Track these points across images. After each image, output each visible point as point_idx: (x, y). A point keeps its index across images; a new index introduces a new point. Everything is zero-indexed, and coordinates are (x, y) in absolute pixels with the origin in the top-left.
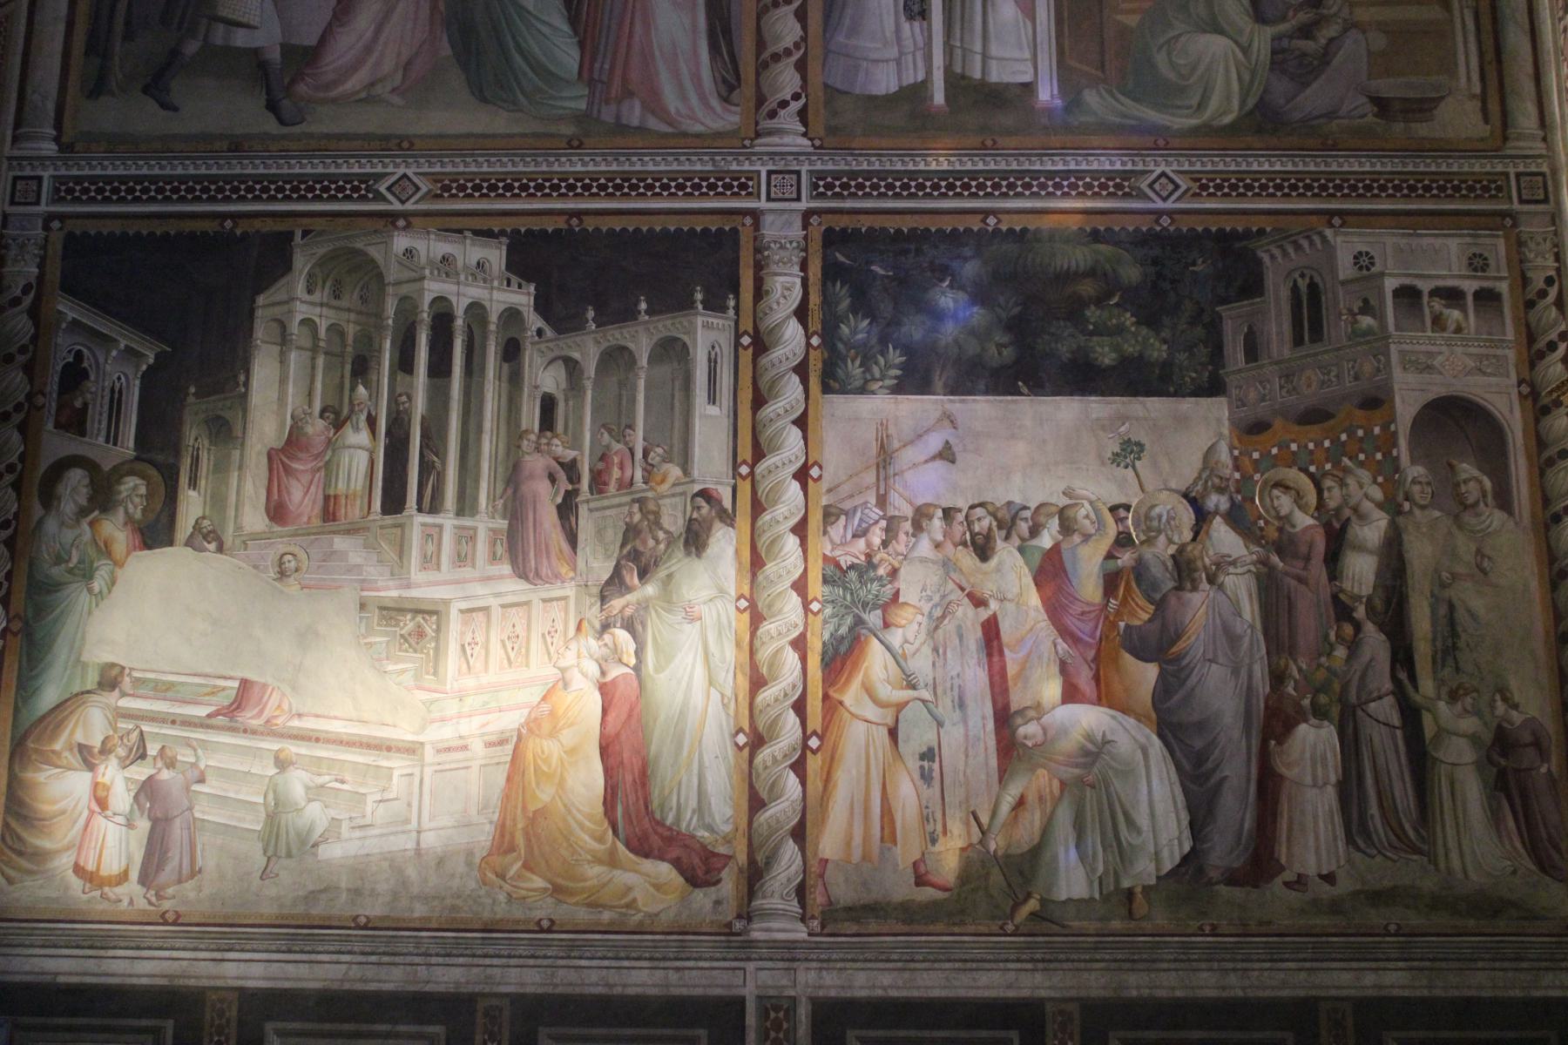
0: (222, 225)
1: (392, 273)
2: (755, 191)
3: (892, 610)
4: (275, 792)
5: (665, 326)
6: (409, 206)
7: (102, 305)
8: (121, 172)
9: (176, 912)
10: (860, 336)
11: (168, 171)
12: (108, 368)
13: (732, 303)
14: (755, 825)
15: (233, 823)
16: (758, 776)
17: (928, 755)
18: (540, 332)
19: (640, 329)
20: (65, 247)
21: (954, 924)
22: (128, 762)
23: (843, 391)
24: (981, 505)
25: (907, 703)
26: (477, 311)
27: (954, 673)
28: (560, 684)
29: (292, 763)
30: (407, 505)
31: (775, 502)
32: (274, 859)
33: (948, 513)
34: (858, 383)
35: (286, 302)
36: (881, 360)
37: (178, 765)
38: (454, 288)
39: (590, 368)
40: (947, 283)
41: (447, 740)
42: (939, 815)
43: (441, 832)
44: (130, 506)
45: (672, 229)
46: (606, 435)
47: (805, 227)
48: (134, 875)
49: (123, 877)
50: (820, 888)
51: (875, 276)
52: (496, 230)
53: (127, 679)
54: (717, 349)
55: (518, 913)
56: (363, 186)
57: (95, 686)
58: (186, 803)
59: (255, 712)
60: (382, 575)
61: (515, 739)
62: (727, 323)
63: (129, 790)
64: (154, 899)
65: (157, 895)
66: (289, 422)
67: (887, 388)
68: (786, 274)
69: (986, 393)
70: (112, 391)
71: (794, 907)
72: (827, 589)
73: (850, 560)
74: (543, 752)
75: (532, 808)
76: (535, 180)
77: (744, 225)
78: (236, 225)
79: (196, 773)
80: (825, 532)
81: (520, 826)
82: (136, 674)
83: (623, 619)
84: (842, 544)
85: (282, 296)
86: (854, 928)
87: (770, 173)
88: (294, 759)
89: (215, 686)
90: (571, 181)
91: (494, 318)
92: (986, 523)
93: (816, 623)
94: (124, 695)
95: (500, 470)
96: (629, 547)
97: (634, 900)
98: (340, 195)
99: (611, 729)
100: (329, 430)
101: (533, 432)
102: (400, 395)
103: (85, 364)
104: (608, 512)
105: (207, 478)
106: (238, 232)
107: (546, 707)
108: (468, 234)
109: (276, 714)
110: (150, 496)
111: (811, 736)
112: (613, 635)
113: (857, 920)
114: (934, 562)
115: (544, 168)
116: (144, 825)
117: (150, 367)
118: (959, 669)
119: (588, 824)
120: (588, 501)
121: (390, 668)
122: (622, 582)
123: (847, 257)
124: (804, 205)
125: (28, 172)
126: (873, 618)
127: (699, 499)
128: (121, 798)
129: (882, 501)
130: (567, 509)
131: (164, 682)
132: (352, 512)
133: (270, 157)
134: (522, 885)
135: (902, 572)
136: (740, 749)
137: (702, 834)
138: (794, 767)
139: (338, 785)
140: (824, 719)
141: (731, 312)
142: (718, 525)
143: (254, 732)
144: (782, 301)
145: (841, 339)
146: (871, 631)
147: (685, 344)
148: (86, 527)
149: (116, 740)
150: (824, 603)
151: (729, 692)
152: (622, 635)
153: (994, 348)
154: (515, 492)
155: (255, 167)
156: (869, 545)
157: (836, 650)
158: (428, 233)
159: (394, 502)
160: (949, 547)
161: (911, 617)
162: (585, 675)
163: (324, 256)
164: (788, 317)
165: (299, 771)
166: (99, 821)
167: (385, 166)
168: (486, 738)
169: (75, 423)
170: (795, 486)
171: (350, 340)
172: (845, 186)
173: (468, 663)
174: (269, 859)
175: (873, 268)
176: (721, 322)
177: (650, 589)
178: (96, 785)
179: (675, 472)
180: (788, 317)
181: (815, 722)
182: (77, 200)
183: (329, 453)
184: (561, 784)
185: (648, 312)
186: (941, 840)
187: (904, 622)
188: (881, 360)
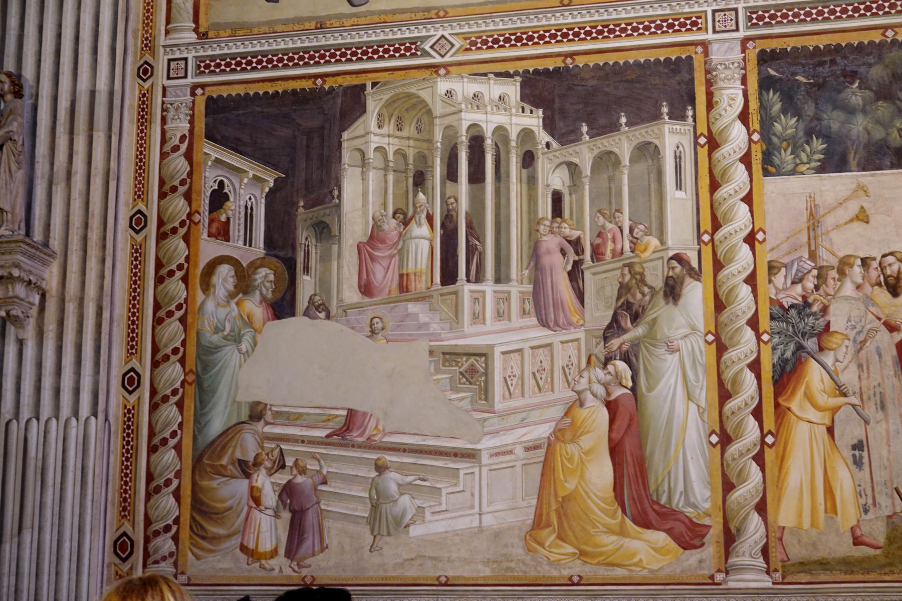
0: (314, 83)
1: (438, 109)
2: (704, 26)
3: (825, 337)
5: (640, 134)
6: (447, 59)
7: (236, 147)
8: (241, 50)
9: (312, 577)
10: (789, 131)
11: (274, 47)
12: (242, 192)
13: (690, 113)
14: (727, 503)
16: (728, 465)
17: (858, 446)
18: (548, 145)
19: (623, 137)
20: (207, 107)
21: (885, 574)
22: (273, 471)
23: (779, 174)
24: (891, 254)
25: (840, 407)
26: (500, 131)
27: (876, 383)
28: (578, 403)
31: (731, 261)
32: (378, 537)
33: (865, 262)
34: (790, 167)
35: (363, 136)
36: (807, 148)
37: (308, 472)
39: (587, 170)
40: (856, 85)
41: (498, 447)
42: (869, 491)
44: (264, 289)
45: (642, 60)
46: (601, 218)
47: (743, 51)
48: (282, 551)
49: (274, 553)
50: (780, 549)
51: (799, 84)
52: (512, 72)
53: (269, 413)
54: (681, 148)
55: (555, 573)
56: (411, 47)
57: (247, 418)
58: (315, 499)
59: (360, 431)
60: (443, 329)
61: (546, 445)
62: (687, 128)
63: (275, 491)
64: (296, 568)
65: (298, 564)
66: (371, 222)
67: (813, 169)
68: (730, 88)
69: (892, 167)
70: (246, 207)
71: (760, 562)
72: (774, 324)
73: (791, 301)
74: (567, 453)
75: (562, 493)
77: (696, 53)
78: (324, 82)
79: (321, 477)
80: (770, 281)
81: (554, 506)
82: (274, 409)
83: (621, 353)
84: (783, 289)
85: (361, 131)
86: (807, 578)
87: (714, 11)
88: (389, 464)
89: (330, 415)
91: (513, 136)
92: (895, 268)
93: (766, 351)
94: (267, 423)
95: (525, 248)
96: (622, 300)
97: (641, 560)
98: (397, 55)
99: (616, 436)
101: (547, 219)
102: (449, 198)
103: (226, 190)
106: (326, 87)
107: (568, 420)
108: (492, 76)
109: (375, 432)
110: (276, 282)
111: (766, 435)
112: (614, 365)
113: (809, 572)
114: (854, 298)
115: (544, 22)
116: (286, 515)
117: (270, 189)
118: (880, 380)
121: (454, 396)
122: (619, 326)
123: (777, 71)
124: (742, 34)
125: (177, 55)
126: (811, 344)
127: (674, 262)
128: (270, 498)
129: (813, 256)
130: (575, 274)
131: (295, 414)
132: (419, 285)
133: (345, 31)
134: (556, 551)
135: (832, 309)
136: (714, 446)
137: (689, 511)
138: (754, 458)
140: (776, 422)
141: (690, 120)
142: (688, 280)
144: (728, 108)
145: (775, 134)
146: (809, 353)
147: (656, 146)
148: (233, 304)
149: (264, 456)
150: (772, 334)
151: (703, 404)
152: (622, 365)
153: (896, 132)
154: (536, 264)
155: (335, 39)
156: (804, 289)
157: (783, 369)
158: (462, 77)
159: (449, 276)
160: (868, 289)
161: (840, 342)
162: (595, 396)
163: (387, 101)
164: (734, 121)
166: (256, 513)
167: (428, 30)
169: (222, 233)
170: (746, 248)
171: (411, 161)
172: (773, 17)
173: (509, 389)
174: (375, 537)
175: (797, 78)
176: (683, 128)
177: (639, 331)
178: (252, 488)
179: (654, 242)
180: (734, 121)
181: (769, 423)
182: (213, 72)
183: (401, 243)
184: (582, 477)
185: (629, 124)
186: (872, 510)
187: (834, 346)
188: (807, 148)
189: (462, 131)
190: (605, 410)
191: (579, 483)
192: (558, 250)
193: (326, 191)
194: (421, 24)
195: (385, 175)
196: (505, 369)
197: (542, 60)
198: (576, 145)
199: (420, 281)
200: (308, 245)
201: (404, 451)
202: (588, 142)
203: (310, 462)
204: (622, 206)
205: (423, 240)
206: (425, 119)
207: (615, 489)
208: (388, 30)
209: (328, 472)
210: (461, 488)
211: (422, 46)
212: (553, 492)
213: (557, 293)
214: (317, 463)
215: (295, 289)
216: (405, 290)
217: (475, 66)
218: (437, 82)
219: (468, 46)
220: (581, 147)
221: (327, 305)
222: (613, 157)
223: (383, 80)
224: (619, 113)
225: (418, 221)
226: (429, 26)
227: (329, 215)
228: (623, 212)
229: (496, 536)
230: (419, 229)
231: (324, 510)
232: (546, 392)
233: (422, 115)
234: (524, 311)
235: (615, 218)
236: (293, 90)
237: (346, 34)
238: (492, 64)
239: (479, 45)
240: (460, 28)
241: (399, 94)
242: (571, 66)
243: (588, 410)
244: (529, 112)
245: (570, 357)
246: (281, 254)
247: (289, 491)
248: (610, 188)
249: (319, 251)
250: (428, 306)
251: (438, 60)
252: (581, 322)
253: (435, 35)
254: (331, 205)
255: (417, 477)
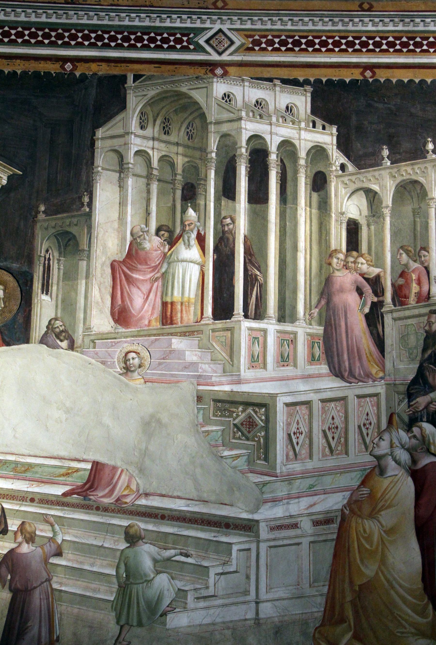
0: (62, 67)
4: (126, 565)
6: (225, 57)
11: (12, 18)
15: (88, 594)
18: (343, 167)
28: (377, 470)
29: (140, 538)
30: (235, 312)
32: (126, 628)
37: (37, 539)
38: (268, 128)
41: (280, 518)
43: (277, 603)
46: (404, 256)
52: (301, 79)
58: (45, 575)
59: (107, 490)
60: (216, 372)
61: (339, 519)
66: (129, 238)
74: (365, 531)
75: (358, 581)
76: (333, 37)
78: (75, 68)
81: (349, 598)
83: (428, 414)
85: (121, 131)
88: (143, 533)
89: (69, 468)
90: (364, 39)
91: (302, 154)
95: (314, 283)
96: (429, 352)
98: (165, 46)
100: (164, 246)
101: (341, 252)
102: (225, 218)
104: (410, 321)
105: (58, 284)
106: (78, 74)
107: (365, 491)
108: (277, 82)
109: (126, 493)
112: (421, 428)
115: (340, 27)
119: (409, 598)
120: (391, 312)
122: (426, 382)
131: (23, 464)
133: (102, 10)
139: (183, 559)
143: (106, 510)
154: (328, 303)
158: (243, 80)
162: (398, 462)
165: (148, 545)
167: (203, 22)
168: (314, 517)
171: (179, 170)
174: (122, 627)
183: (165, 266)
184: (383, 561)
189: (241, 142)
190: (410, 479)
191: (379, 567)
192: (354, 288)
193: (75, 196)
194: (194, 13)
195: (148, 184)
196: (289, 424)
197: (337, 70)
198: (375, 170)
199: (188, 312)
200: (49, 259)
201: (163, 517)
202: (388, 168)
203: (41, 527)
204: (428, 244)
205: (192, 265)
206: (198, 122)
207: (424, 579)
208: (155, 15)
209: (63, 540)
210: (232, 569)
211: (196, 40)
212: (347, 580)
213: (352, 340)
214: (50, 528)
215: (30, 311)
216: (169, 322)
217: (259, 69)
218: (213, 82)
219: (251, 46)
220: (383, 172)
221: (70, 332)
222: (418, 188)
223: (148, 74)
224: (425, 139)
225: (186, 241)
226: (204, 17)
227: (76, 225)
228: (430, 251)
229: (276, 633)
230: (188, 250)
231: (56, 590)
232: (338, 454)
233: (194, 119)
234: (313, 356)
235: (420, 257)
236: (35, 72)
237: (104, 14)
238: (279, 69)
239: (264, 45)
240: (241, 24)
241: (166, 92)
242: (371, 80)
243: (390, 479)
244: (321, 128)
245: (367, 414)
246: (15, 266)
247: (10, 564)
248: (415, 222)
249: (62, 267)
250: (197, 342)
251: (215, 57)
252: (381, 374)
253: (211, 28)
254: (79, 213)
255: (179, 551)
